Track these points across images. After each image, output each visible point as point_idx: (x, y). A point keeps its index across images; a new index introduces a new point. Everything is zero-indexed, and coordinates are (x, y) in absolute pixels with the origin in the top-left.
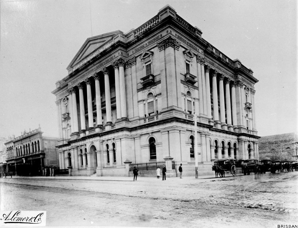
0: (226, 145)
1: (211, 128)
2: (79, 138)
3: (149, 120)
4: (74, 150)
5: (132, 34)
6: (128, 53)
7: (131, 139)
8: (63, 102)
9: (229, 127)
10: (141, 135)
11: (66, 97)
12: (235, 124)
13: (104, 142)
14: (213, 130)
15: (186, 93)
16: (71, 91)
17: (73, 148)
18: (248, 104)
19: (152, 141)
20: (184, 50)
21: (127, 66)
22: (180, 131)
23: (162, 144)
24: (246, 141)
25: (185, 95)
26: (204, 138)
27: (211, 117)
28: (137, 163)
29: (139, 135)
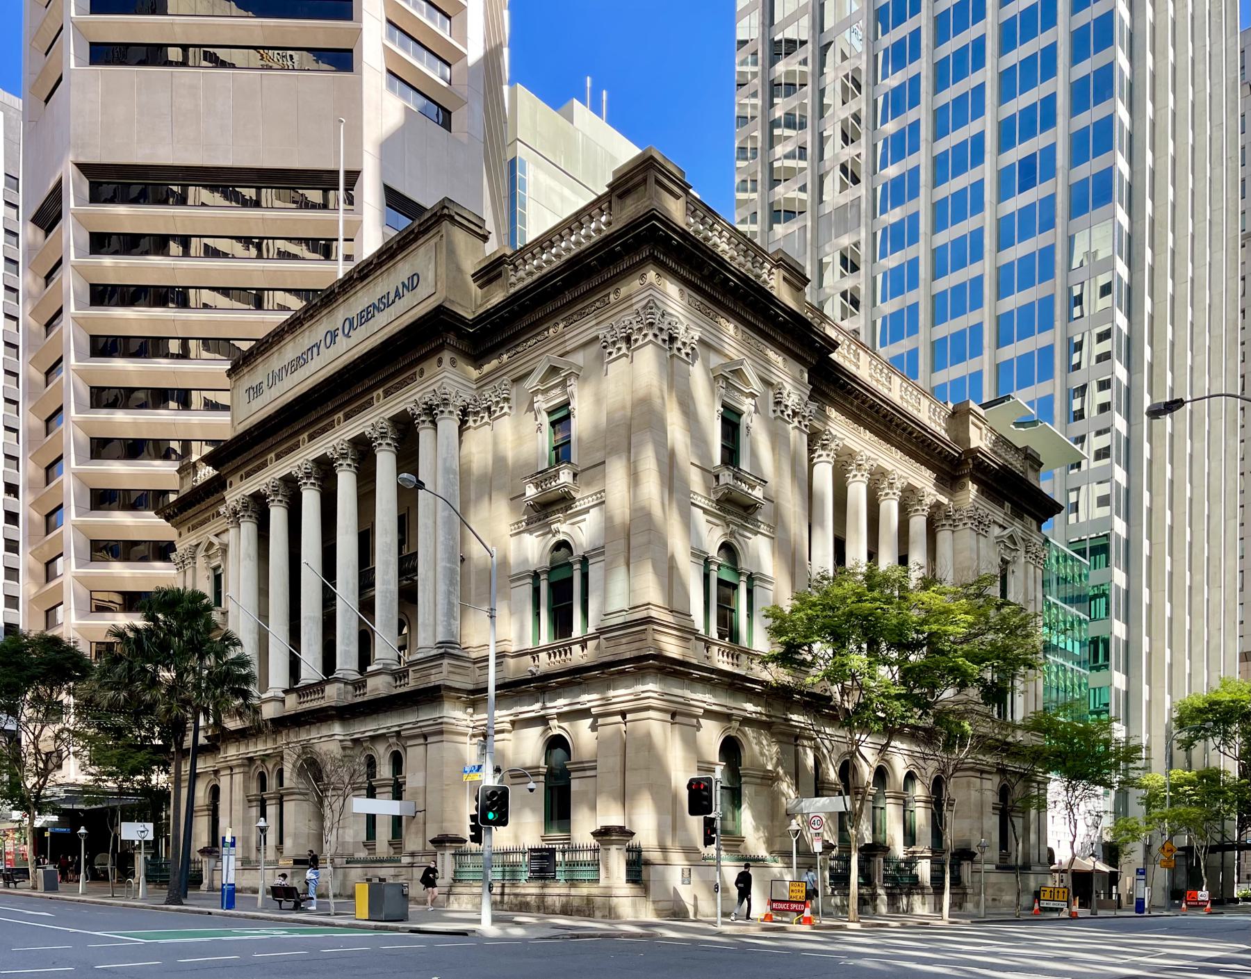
11: (217, 535)
21: (471, 419)
23: (595, 768)
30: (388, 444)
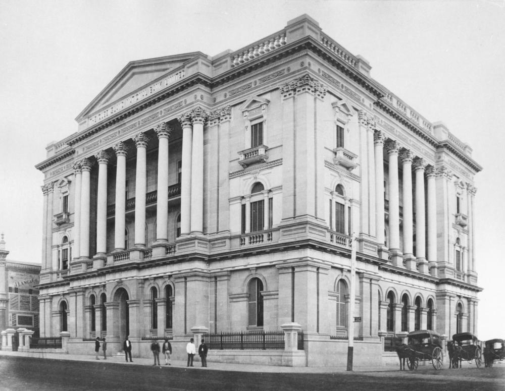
0: (412, 300)
1: (382, 264)
2: (89, 270)
3: (252, 241)
4: (76, 296)
5: (226, 61)
6: (214, 96)
7: (207, 280)
8: (60, 189)
9: (420, 265)
10: (231, 271)
11: (66, 177)
12: (433, 257)
13: (147, 283)
14: (385, 270)
15: (333, 188)
16: (80, 167)
17: (75, 290)
18: (460, 218)
19: (257, 284)
20: (334, 99)
21: (209, 122)
22: (318, 268)
24: (452, 295)
25: (331, 193)
26: (366, 286)
27: (381, 239)
28: (219, 332)
29: (227, 271)
30: (165, 134)
